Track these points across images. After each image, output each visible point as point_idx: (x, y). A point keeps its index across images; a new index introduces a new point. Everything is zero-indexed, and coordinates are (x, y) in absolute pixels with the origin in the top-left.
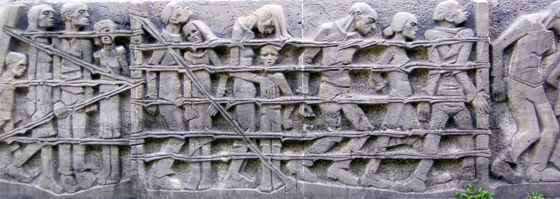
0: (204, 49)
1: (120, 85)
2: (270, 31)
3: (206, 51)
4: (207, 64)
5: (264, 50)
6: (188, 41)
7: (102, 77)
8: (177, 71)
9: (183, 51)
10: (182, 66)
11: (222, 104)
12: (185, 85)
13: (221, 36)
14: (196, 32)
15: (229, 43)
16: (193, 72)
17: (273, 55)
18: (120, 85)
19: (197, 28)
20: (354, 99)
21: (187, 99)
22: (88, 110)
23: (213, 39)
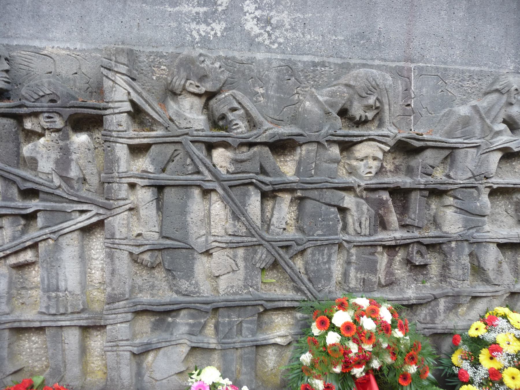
0: (251, 145)
1: (82, 212)
2: (370, 115)
3: (255, 149)
4: (257, 174)
5: (361, 150)
6: (221, 128)
7: (41, 195)
8: (199, 186)
9: (210, 147)
10: (210, 177)
11: (282, 247)
12: (213, 212)
13: (278, 122)
14: (237, 112)
15: (301, 135)
16: (230, 187)
17: (375, 159)
18: (82, 212)
19: (240, 103)
20: (495, 236)
21: (219, 239)
22: (13, 260)
23: (271, 130)
